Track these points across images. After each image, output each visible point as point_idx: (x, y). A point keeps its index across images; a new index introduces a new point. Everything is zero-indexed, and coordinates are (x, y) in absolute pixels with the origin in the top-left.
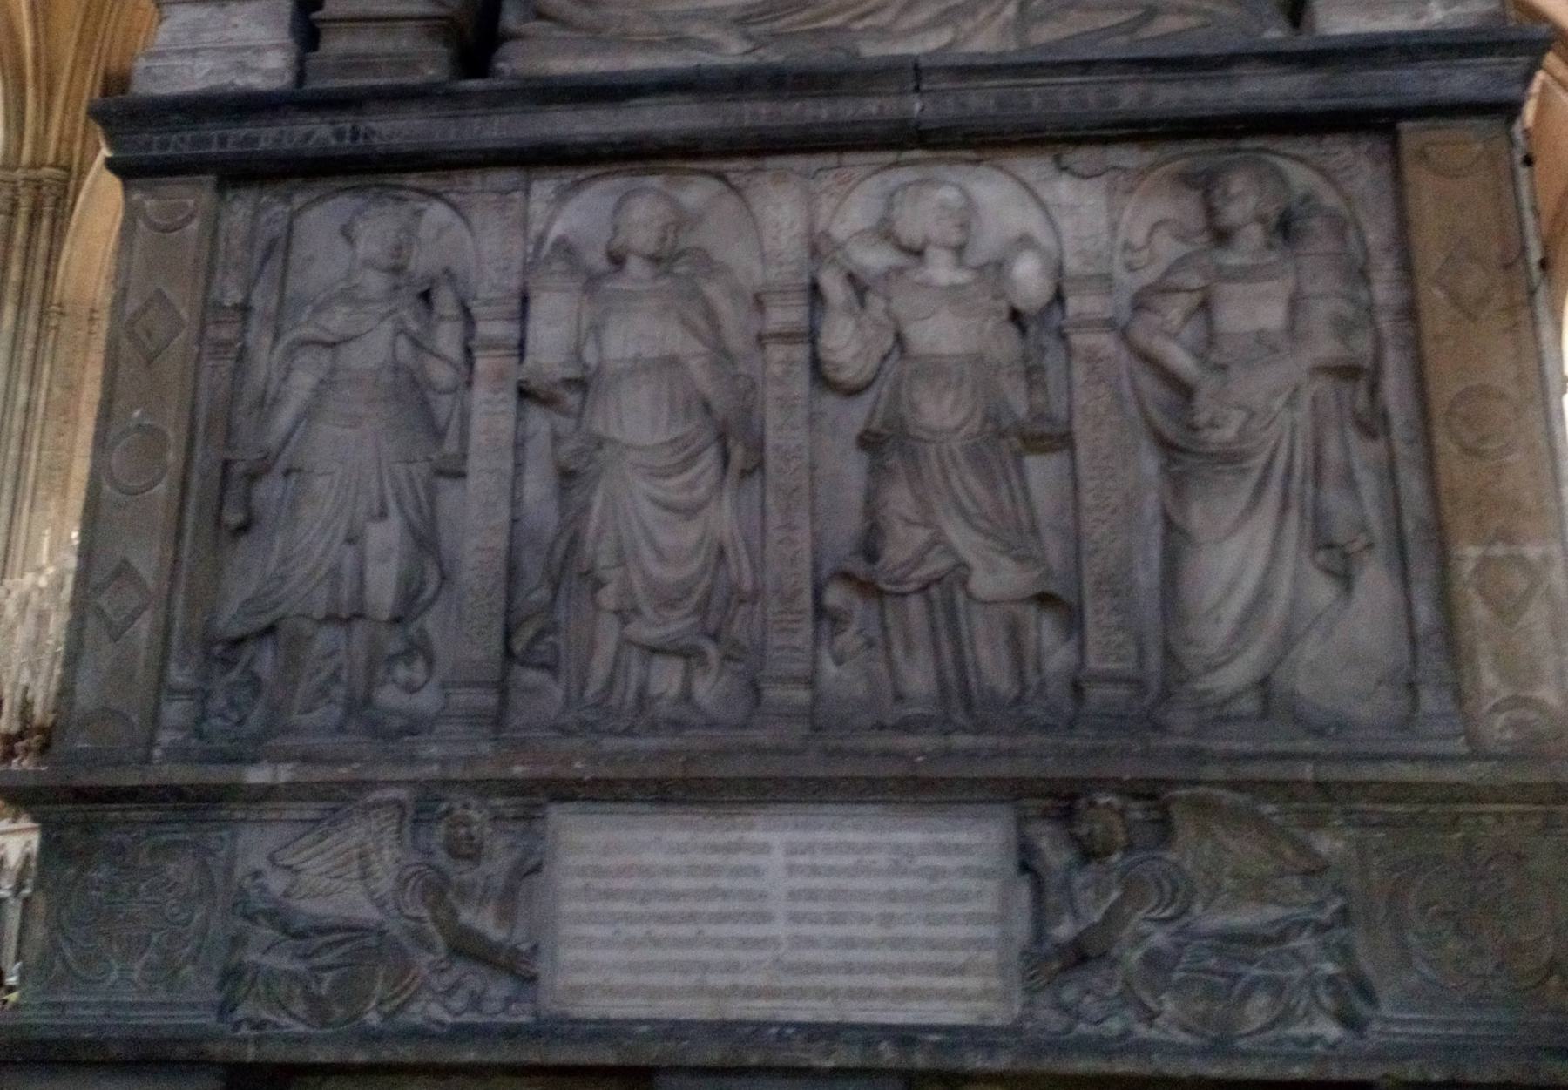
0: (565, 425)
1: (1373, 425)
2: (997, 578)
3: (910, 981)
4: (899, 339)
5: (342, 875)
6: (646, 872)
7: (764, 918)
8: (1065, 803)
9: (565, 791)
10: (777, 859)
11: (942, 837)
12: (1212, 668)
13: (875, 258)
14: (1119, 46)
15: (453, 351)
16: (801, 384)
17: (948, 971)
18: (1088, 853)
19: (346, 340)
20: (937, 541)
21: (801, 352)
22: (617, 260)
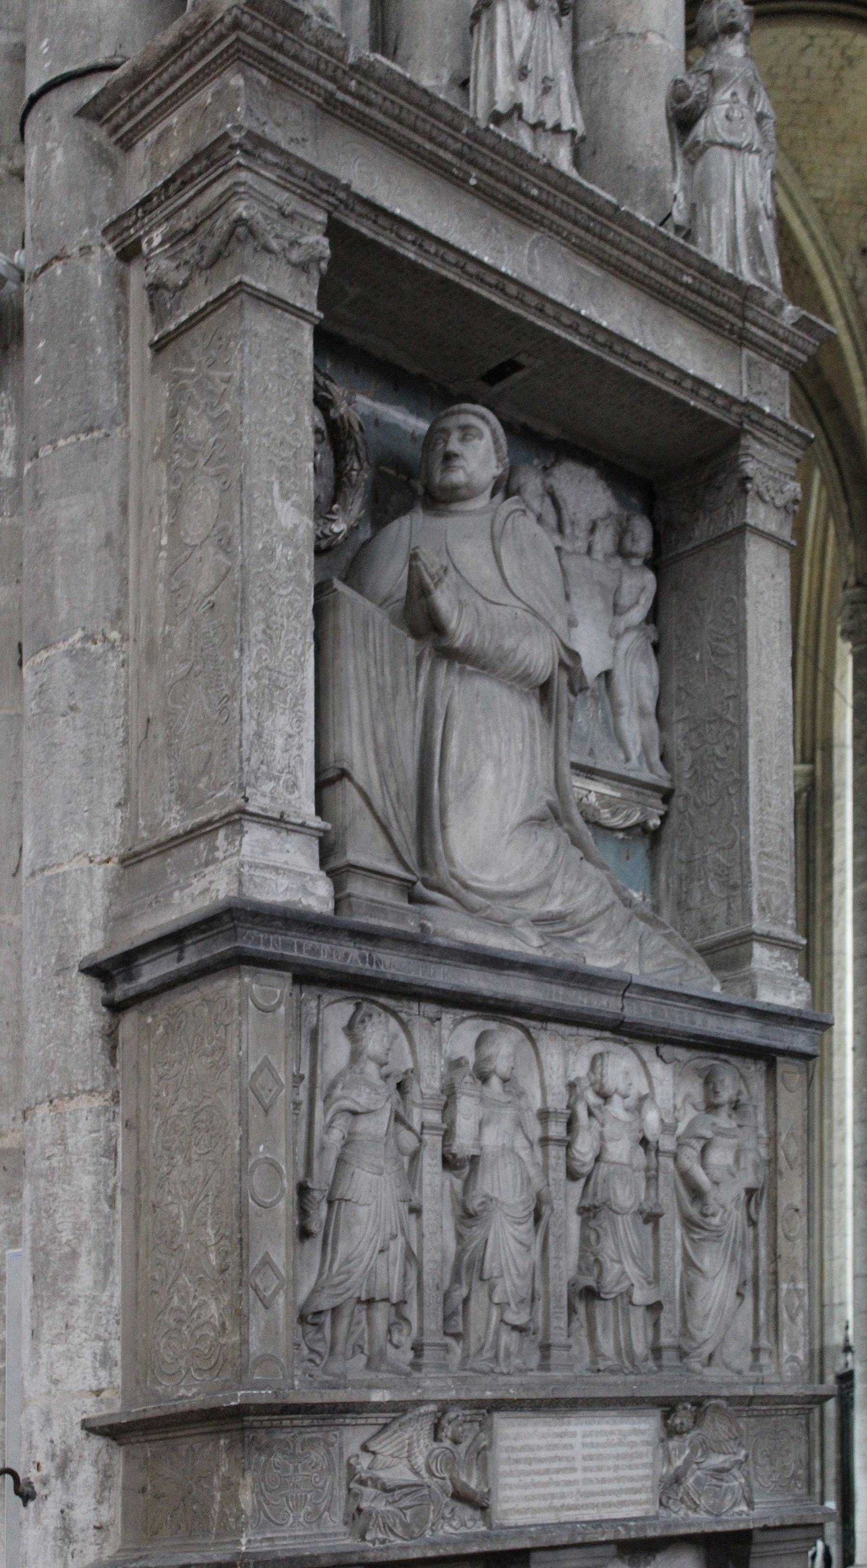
3: (624, 1497)
6: (531, 1449)
7: (573, 1470)
10: (579, 1439)
11: (636, 1426)
19: (369, 1112)
20: (623, 1272)
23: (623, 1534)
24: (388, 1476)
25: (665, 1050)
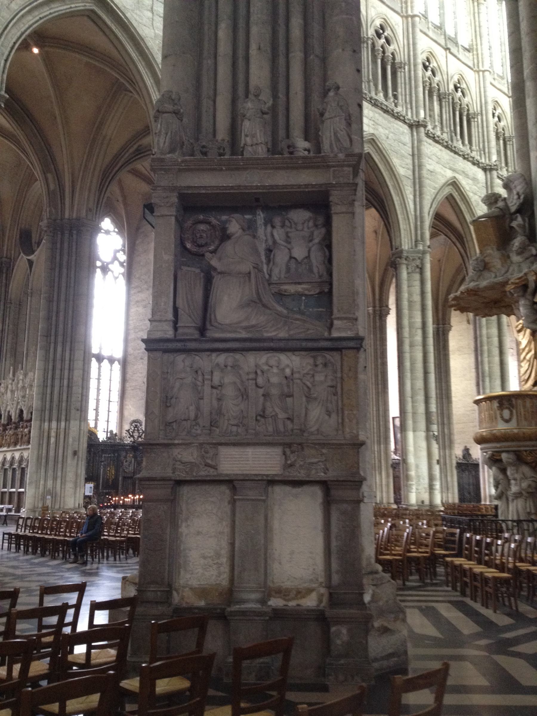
0: (218, 392)
1: (335, 394)
2: (282, 415)
4: (269, 380)
5: (190, 455)
8: (289, 445)
9: (221, 444)
10: (250, 453)
12: (311, 428)
13: (265, 368)
14: (302, 336)
15: (202, 381)
16: (254, 387)
17: (272, 467)
18: (293, 452)
20: (274, 410)
21: (254, 382)
22: (226, 366)
23: (269, 478)
24: (185, 460)
25: (296, 353)
